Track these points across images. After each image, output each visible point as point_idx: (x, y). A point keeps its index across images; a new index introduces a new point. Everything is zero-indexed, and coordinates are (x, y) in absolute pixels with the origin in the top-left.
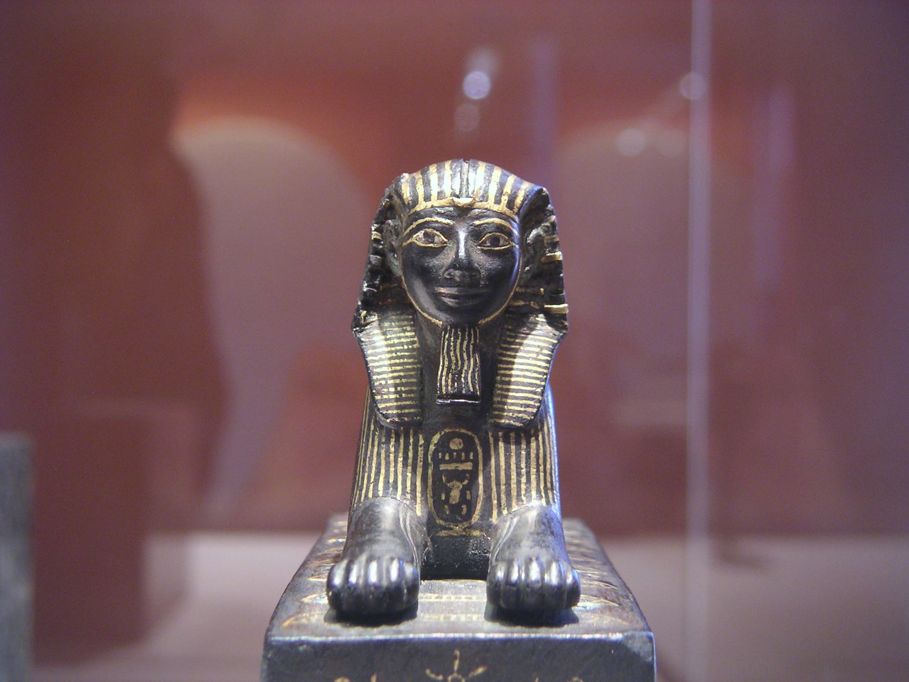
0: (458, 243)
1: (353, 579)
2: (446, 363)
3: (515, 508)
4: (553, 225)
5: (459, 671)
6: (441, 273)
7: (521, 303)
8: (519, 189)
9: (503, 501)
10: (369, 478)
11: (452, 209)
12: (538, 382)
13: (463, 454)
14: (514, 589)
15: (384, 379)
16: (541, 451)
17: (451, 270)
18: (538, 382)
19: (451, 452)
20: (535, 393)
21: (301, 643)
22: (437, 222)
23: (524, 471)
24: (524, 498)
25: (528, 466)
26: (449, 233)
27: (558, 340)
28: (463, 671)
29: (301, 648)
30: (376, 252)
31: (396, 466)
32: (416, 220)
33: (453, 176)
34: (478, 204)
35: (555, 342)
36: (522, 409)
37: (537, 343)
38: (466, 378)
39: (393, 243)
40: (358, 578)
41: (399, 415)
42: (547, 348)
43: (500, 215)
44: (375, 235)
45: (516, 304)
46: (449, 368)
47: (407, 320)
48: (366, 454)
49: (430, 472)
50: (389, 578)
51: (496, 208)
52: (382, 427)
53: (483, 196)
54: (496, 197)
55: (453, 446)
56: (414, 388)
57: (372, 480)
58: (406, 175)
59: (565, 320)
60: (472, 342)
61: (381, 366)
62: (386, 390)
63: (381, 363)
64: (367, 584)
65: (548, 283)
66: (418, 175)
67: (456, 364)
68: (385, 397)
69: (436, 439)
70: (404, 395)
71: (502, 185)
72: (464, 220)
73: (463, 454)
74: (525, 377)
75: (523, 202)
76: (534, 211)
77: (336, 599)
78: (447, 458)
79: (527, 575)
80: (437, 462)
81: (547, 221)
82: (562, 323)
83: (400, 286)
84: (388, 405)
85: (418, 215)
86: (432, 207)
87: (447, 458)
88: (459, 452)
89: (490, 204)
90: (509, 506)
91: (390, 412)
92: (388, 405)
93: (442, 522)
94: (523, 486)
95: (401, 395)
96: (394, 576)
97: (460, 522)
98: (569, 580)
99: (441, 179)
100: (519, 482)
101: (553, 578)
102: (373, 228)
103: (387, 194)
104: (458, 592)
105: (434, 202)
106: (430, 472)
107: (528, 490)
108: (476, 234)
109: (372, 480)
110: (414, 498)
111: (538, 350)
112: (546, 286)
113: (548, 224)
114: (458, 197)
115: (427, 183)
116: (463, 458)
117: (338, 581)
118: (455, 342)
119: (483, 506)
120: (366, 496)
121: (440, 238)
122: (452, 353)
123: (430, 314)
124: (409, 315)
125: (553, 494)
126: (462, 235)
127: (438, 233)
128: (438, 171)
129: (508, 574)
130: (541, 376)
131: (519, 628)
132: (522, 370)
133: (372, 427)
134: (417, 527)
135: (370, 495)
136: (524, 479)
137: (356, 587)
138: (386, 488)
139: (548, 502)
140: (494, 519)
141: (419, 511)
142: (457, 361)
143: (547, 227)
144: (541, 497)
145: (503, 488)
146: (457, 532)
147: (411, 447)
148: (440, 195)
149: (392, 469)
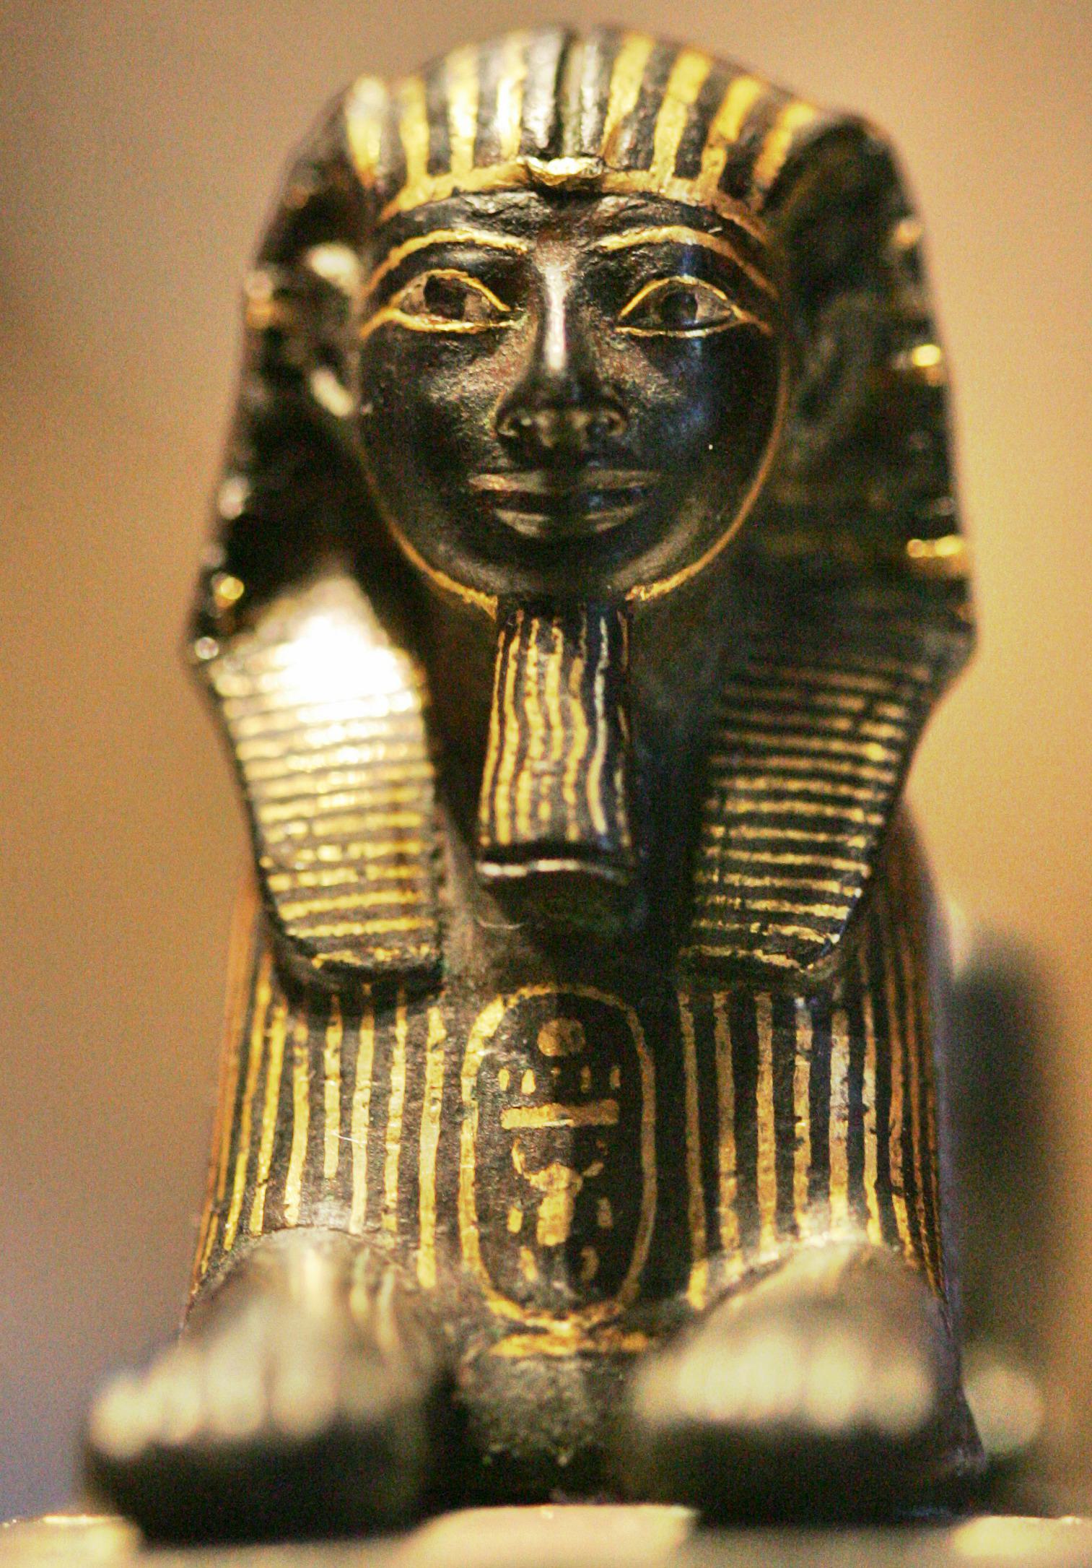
2: (513, 737)
15: (299, 818)
22: (471, 245)
23: (803, 1128)
26: (513, 280)
31: (345, 1123)
32: (399, 242)
43: (693, 216)
49: (468, 1136)
51: (681, 191)
54: (680, 154)
57: (263, 1172)
62: (307, 856)
68: (307, 880)
72: (566, 236)
80: (492, 1104)
84: (318, 905)
85: (406, 226)
89: (660, 176)
91: (323, 931)
95: (361, 873)
105: (464, 175)
106: (468, 1136)
109: (263, 1172)
110: (410, 1227)
114: (545, 156)
127: (475, 283)
142: (548, 726)
144: (866, 1214)
146: (563, 1342)
147: (399, 1053)
149: (332, 1133)
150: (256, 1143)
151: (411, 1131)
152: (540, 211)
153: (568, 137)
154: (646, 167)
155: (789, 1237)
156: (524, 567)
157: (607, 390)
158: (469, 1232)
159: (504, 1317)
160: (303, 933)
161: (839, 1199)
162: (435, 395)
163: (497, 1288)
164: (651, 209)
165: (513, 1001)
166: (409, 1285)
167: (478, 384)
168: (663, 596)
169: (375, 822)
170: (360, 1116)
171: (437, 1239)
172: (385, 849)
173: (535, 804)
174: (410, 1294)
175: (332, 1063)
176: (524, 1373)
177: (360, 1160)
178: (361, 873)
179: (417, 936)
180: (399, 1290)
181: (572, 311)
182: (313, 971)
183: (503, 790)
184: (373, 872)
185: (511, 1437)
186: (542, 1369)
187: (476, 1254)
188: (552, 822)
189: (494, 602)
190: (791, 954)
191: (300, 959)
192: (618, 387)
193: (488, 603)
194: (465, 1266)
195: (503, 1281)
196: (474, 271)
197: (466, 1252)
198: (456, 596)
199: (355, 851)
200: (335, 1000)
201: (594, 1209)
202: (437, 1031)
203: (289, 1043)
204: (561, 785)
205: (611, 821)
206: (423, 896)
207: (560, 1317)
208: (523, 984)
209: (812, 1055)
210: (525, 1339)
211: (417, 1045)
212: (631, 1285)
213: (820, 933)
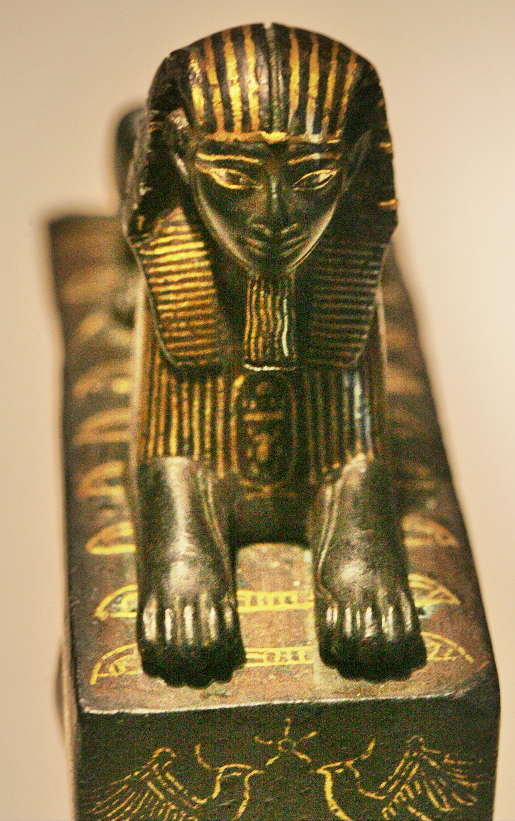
2: (255, 322)
49: (233, 423)
62: (174, 325)
67: (268, 324)
68: (175, 334)
80: (241, 412)
106: (233, 423)
122: (262, 312)
147: (208, 394)
149: (186, 422)
151: (213, 424)
158: (234, 457)
173: (265, 347)
203: (169, 384)
212: (289, 475)
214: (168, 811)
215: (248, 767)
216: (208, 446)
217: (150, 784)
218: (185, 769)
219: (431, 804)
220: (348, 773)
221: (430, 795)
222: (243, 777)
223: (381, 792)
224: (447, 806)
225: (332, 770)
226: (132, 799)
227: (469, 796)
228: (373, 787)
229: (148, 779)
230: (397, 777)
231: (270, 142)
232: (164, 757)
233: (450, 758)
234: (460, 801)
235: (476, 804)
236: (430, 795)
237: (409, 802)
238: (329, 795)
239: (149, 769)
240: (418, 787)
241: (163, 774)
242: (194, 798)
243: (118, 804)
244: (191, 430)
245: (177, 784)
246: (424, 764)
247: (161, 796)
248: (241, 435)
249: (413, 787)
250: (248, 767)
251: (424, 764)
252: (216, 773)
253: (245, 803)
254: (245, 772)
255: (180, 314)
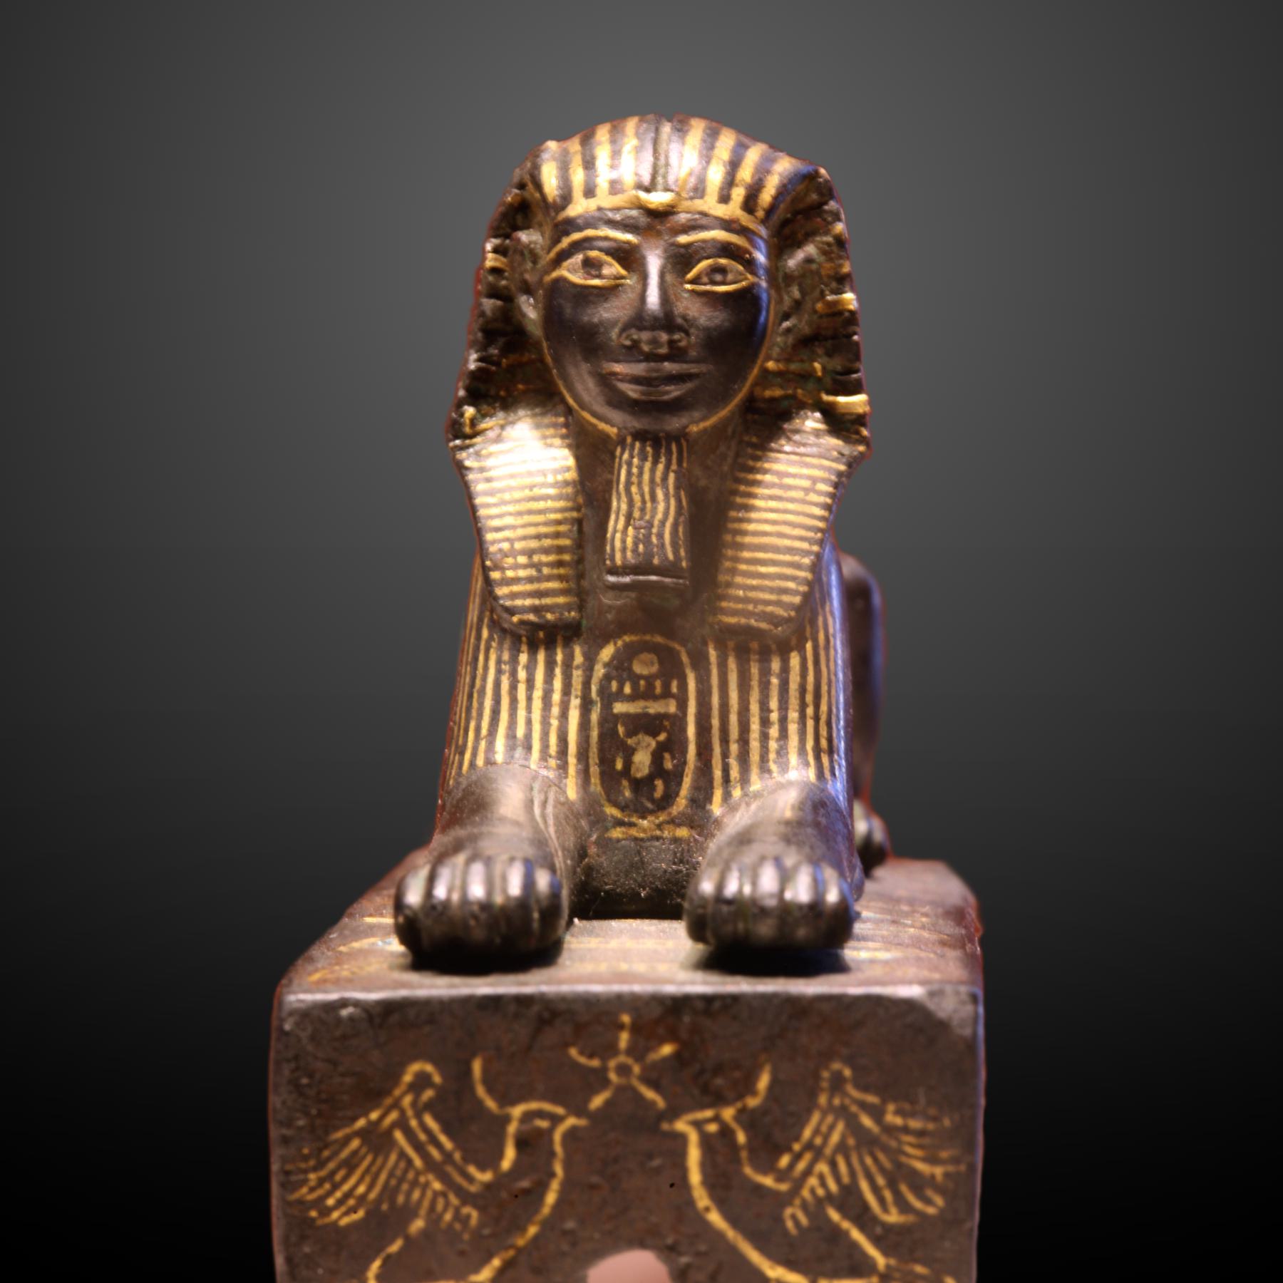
0: (644, 278)
1: (440, 892)
2: (624, 507)
3: (756, 785)
4: (840, 242)
5: (630, 1051)
6: (614, 334)
7: (778, 392)
8: (768, 172)
9: (735, 773)
10: (478, 729)
11: (634, 213)
12: (805, 545)
13: (658, 684)
14: (732, 908)
15: (507, 540)
16: (811, 678)
17: (633, 330)
18: (805, 545)
19: (635, 679)
20: (798, 566)
21: (344, 1003)
22: (606, 238)
23: (774, 716)
24: (773, 767)
25: (784, 707)
26: (628, 257)
27: (849, 465)
28: (636, 1051)
29: (345, 1013)
30: (494, 293)
31: (529, 709)
32: (567, 234)
33: (638, 150)
34: (686, 204)
35: (842, 468)
36: (773, 597)
37: (805, 471)
38: (660, 536)
39: (527, 276)
40: (450, 890)
41: (536, 610)
42: (824, 481)
43: (728, 225)
44: (491, 261)
45: (768, 393)
46: (629, 517)
47: (555, 425)
48: (472, 685)
49: (594, 717)
50: (504, 890)
51: (721, 211)
52: (504, 631)
53: (696, 189)
54: (722, 189)
55: (638, 668)
56: (567, 557)
57: (484, 732)
58: (552, 145)
59: (864, 425)
60: (674, 467)
61: (500, 516)
62: (510, 560)
63: (504, 509)
64: (465, 901)
65: (829, 354)
66: (574, 145)
67: (643, 510)
68: (510, 574)
69: (607, 653)
70: (546, 571)
71: (734, 165)
72: (659, 234)
73: (658, 684)
74: (781, 535)
75: (776, 198)
76: (796, 215)
77: (409, 930)
78: (627, 690)
79: (754, 884)
80: (608, 698)
81: (827, 232)
82: (858, 433)
83: (542, 360)
84: (516, 588)
85: (570, 225)
86: (600, 209)
87: (627, 690)
88: (650, 679)
89: (710, 204)
90: (745, 781)
91: (519, 602)
92: (516, 588)
93: (615, 812)
94: (773, 745)
95: (539, 571)
96: (515, 889)
97: (652, 812)
98: (832, 897)
99: (616, 154)
100: (765, 737)
101: (800, 892)
102: (489, 247)
103: (516, 179)
104: (637, 935)
105: (604, 199)
106: (594, 717)
107: (782, 752)
108: (681, 260)
109: (484, 732)
110: (563, 767)
111: (806, 483)
112: (825, 359)
113: (829, 239)
114: (648, 190)
115: (589, 164)
116: (658, 690)
117: (414, 897)
118: (641, 469)
119: (695, 781)
120: (472, 764)
121: (613, 268)
122: (634, 489)
123: (594, 414)
124: (557, 415)
125: (831, 761)
126: (654, 263)
127: (609, 259)
128: (613, 141)
129: (720, 886)
130: (811, 534)
131: (739, 979)
132: (774, 522)
133: (485, 633)
134: (567, 818)
135: (480, 762)
136: (774, 731)
137: (446, 904)
138: (511, 747)
139: (820, 774)
140: (716, 808)
141: (572, 791)
142: (644, 502)
143: (828, 244)
144: (807, 764)
145: (734, 748)
146: (644, 831)
147: (558, 671)
148: (615, 187)
149: (521, 713)
150: (480, 715)
151: (564, 715)
152: (644, 220)
153: (660, 180)
154: (702, 197)
155: (767, 776)
156: (633, 413)
157: (679, 321)
158: (594, 770)
159: (612, 816)
160: (508, 603)
161: (793, 758)
162: (586, 319)
163: (609, 801)
164: (704, 221)
165: (620, 643)
166: (562, 799)
167: (611, 313)
168: (705, 430)
169: (547, 542)
170: (537, 704)
171: (578, 772)
172: (551, 558)
173: (636, 544)
174: (563, 804)
175: (522, 675)
176: (623, 847)
177: (537, 728)
178: (539, 571)
179: (569, 607)
180: (558, 803)
181: (662, 276)
182: (512, 623)
183: (618, 536)
184: (546, 571)
185: (615, 883)
186: (633, 844)
187: (598, 781)
188: (645, 553)
189: (615, 430)
190: (770, 622)
191: (505, 615)
192: (684, 318)
193: (613, 431)
194: (592, 788)
195: (613, 797)
196: (608, 252)
197: (593, 780)
198: (594, 426)
199: (536, 558)
200: (524, 639)
201: (662, 758)
202: (579, 658)
204: (650, 534)
205: (676, 552)
206: (573, 585)
207: (644, 818)
208: (625, 633)
209: (780, 676)
210: (623, 829)
211: (568, 666)
213: (786, 610)
214: (429, 1194)
215: (560, 1110)
216: (553, 749)
217: (399, 1135)
218: (455, 1108)
219: (866, 1207)
220: (726, 1132)
221: (864, 1186)
222: (550, 1131)
223: (781, 1176)
224: (893, 1210)
225: (698, 1125)
226: (367, 1170)
227: (930, 1193)
228: (768, 1166)
229: (394, 1125)
230: (809, 1146)
231: (652, 206)
232: (422, 1081)
233: (898, 1112)
234: (918, 1205)
235: (942, 1211)
236: (864, 1186)
237: (829, 1197)
238: (695, 1177)
239: (396, 1105)
240: (843, 1167)
241: (418, 1116)
242: (472, 1170)
243: (345, 1179)
244: (529, 722)
245: (443, 1139)
246: (854, 1126)
247: (418, 1162)
248: (608, 735)
249: (833, 1165)
250: (560, 1110)
251: (854, 1126)
252: (506, 1119)
253: (555, 1185)
254: (556, 1120)
255: (518, 545)
